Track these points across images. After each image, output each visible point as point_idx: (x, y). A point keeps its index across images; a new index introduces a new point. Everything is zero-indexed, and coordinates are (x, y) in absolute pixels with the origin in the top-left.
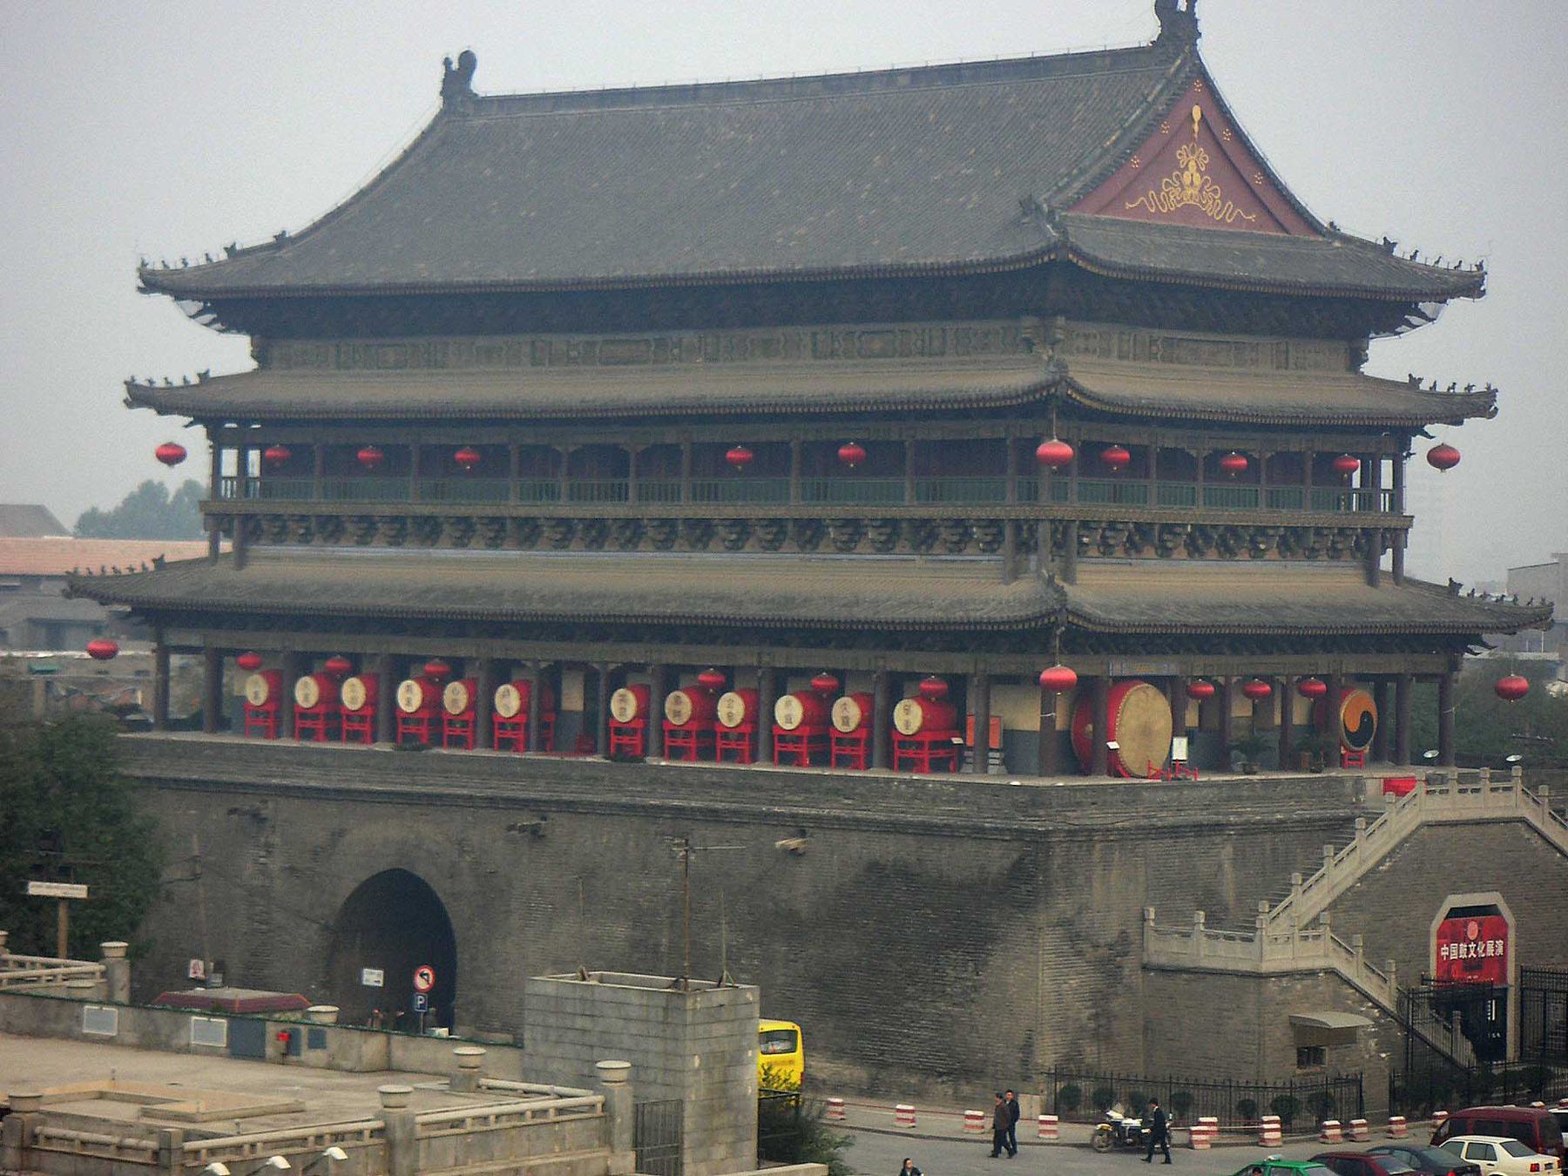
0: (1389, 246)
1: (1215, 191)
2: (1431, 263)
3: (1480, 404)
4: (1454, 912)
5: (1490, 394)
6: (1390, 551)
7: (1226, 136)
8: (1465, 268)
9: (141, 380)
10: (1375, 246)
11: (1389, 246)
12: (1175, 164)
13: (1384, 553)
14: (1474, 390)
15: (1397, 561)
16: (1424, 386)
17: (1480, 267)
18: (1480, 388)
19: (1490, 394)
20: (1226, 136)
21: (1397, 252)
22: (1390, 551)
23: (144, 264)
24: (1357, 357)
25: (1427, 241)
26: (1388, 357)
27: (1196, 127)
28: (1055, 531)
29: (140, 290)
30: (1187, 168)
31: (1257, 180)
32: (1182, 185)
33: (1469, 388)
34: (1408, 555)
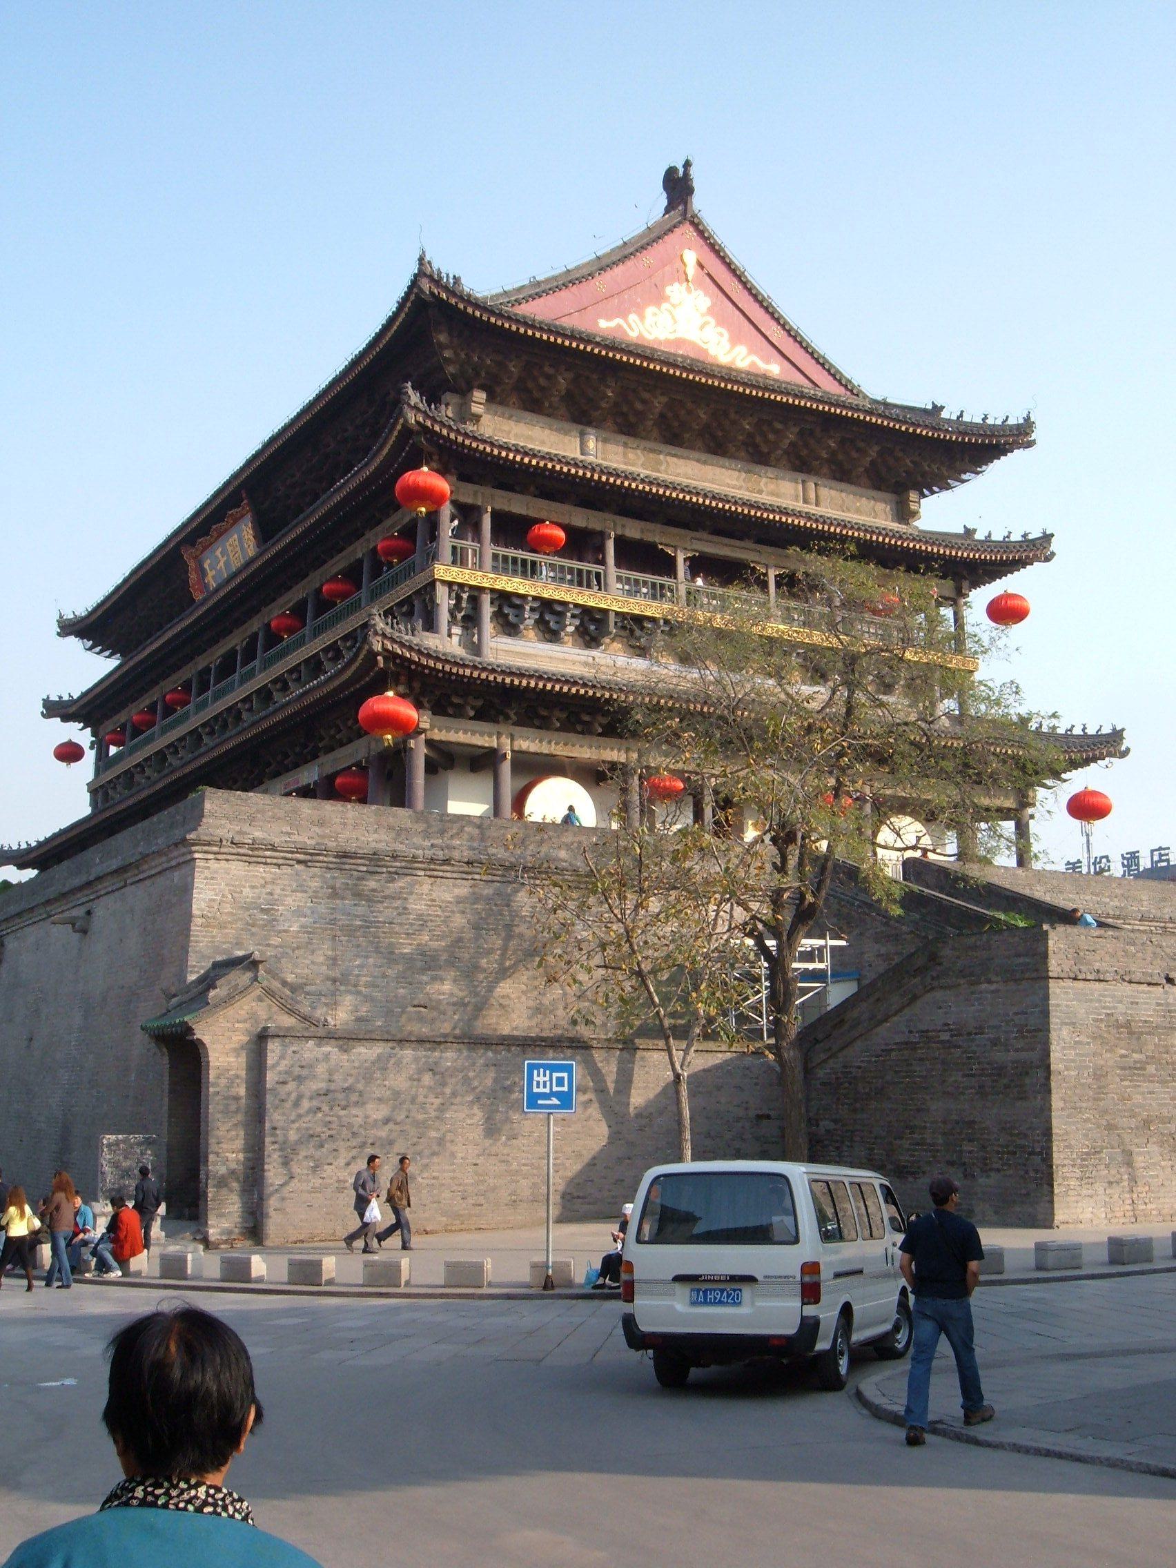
0: (937, 409)
2: (978, 420)
3: (1033, 550)
5: (1047, 538)
8: (1011, 422)
9: (54, 698)
10: (925, 411)
11: (937, 409)
14: (1030, 537)
16: (980, 536)
17: (1027, 419)
18: (1035, 534)
19: (1047, 538)
21: (945, 414)
23: (61, 617)
24: (905, 514)
25: (970, 402)
26: (942, 513)
28: (459, 599)
29: (59, 634)
33: (1025, 536)
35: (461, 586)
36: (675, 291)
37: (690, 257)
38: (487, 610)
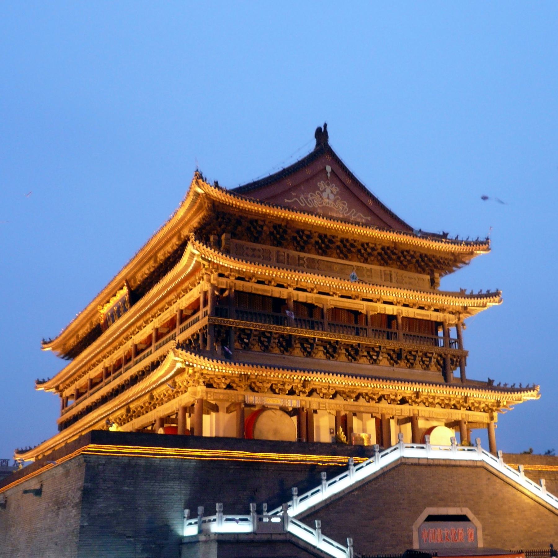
1: (344, 204)
4: (431, 518)
6: (458, 368)
7: (348, 181)
12: (319, 189)
13: (455, 369)
14: (490, 292)
15: (462, 372)
20: (348, 181)
22: (458, 368)
27: (329, 175)
30: (325, 190)
31: (370, 202)
32: (321, 197)
33: (488, 291)
34: (467, 369)
35: (221, 326)
36: (321, 185)
37: (329, 169)
38: (234, 337)
